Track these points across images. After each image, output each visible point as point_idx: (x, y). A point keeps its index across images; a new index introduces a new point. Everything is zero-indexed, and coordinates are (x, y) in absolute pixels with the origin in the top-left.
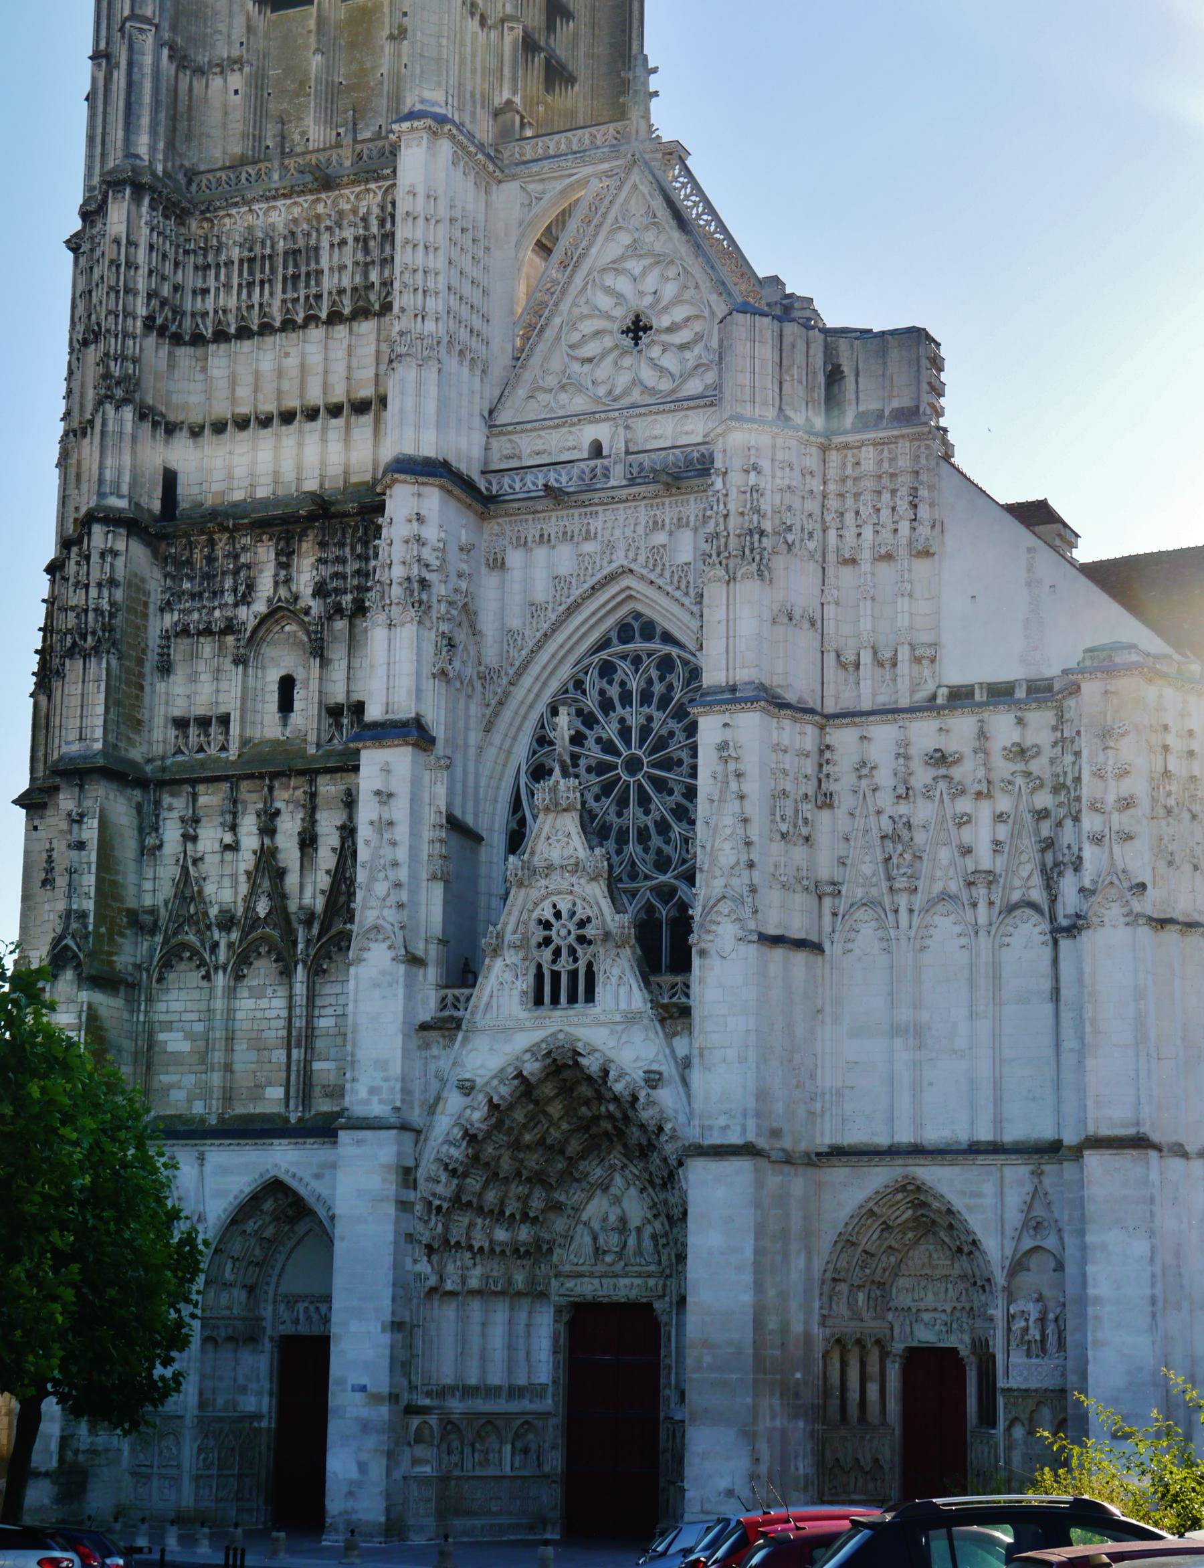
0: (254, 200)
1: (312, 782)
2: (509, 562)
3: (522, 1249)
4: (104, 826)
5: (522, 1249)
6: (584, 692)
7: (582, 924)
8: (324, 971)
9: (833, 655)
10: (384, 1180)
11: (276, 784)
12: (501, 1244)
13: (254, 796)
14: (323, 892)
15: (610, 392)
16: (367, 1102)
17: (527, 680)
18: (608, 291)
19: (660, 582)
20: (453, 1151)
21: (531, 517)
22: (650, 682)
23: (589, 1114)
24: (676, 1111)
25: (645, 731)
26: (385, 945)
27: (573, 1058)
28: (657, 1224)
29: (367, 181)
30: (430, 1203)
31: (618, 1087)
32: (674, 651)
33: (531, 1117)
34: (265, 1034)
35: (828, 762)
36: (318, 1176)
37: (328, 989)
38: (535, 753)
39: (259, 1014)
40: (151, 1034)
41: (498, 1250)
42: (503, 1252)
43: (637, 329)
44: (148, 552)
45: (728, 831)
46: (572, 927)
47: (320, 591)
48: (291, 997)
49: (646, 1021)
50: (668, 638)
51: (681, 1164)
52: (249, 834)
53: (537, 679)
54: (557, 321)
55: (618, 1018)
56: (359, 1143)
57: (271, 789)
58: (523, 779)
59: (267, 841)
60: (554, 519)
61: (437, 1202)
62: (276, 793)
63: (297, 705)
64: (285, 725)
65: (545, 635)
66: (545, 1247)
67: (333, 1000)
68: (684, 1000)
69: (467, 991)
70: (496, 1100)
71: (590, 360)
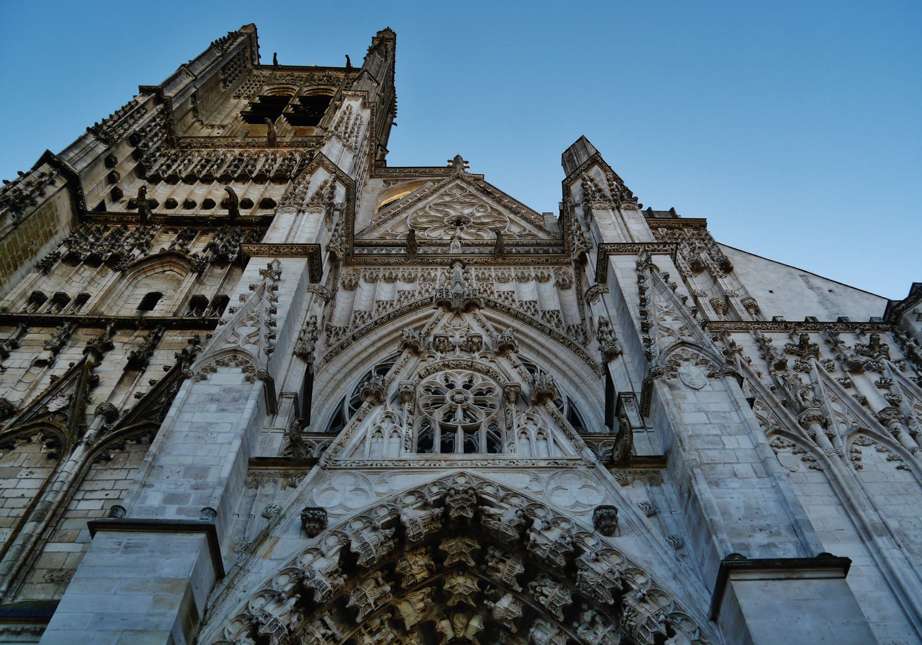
0: (218, 146)
10: (157, 601)
17: (365, 342)
18: (438, 211)
20: (271, 608)
23: (450, 634)
24: (649, 563)
26: (239, 370)
29: (298, 147)
37: (107, 475)
43: (459, 222)
44: (70, 216)
46: (472, 396)
49: (582, 469)
53: (373, 344)
54: (404, 215)
55: (543, 464)
60: (401, 270)
67: (108, 486)
70: (355, 546)
71: (425, 229)
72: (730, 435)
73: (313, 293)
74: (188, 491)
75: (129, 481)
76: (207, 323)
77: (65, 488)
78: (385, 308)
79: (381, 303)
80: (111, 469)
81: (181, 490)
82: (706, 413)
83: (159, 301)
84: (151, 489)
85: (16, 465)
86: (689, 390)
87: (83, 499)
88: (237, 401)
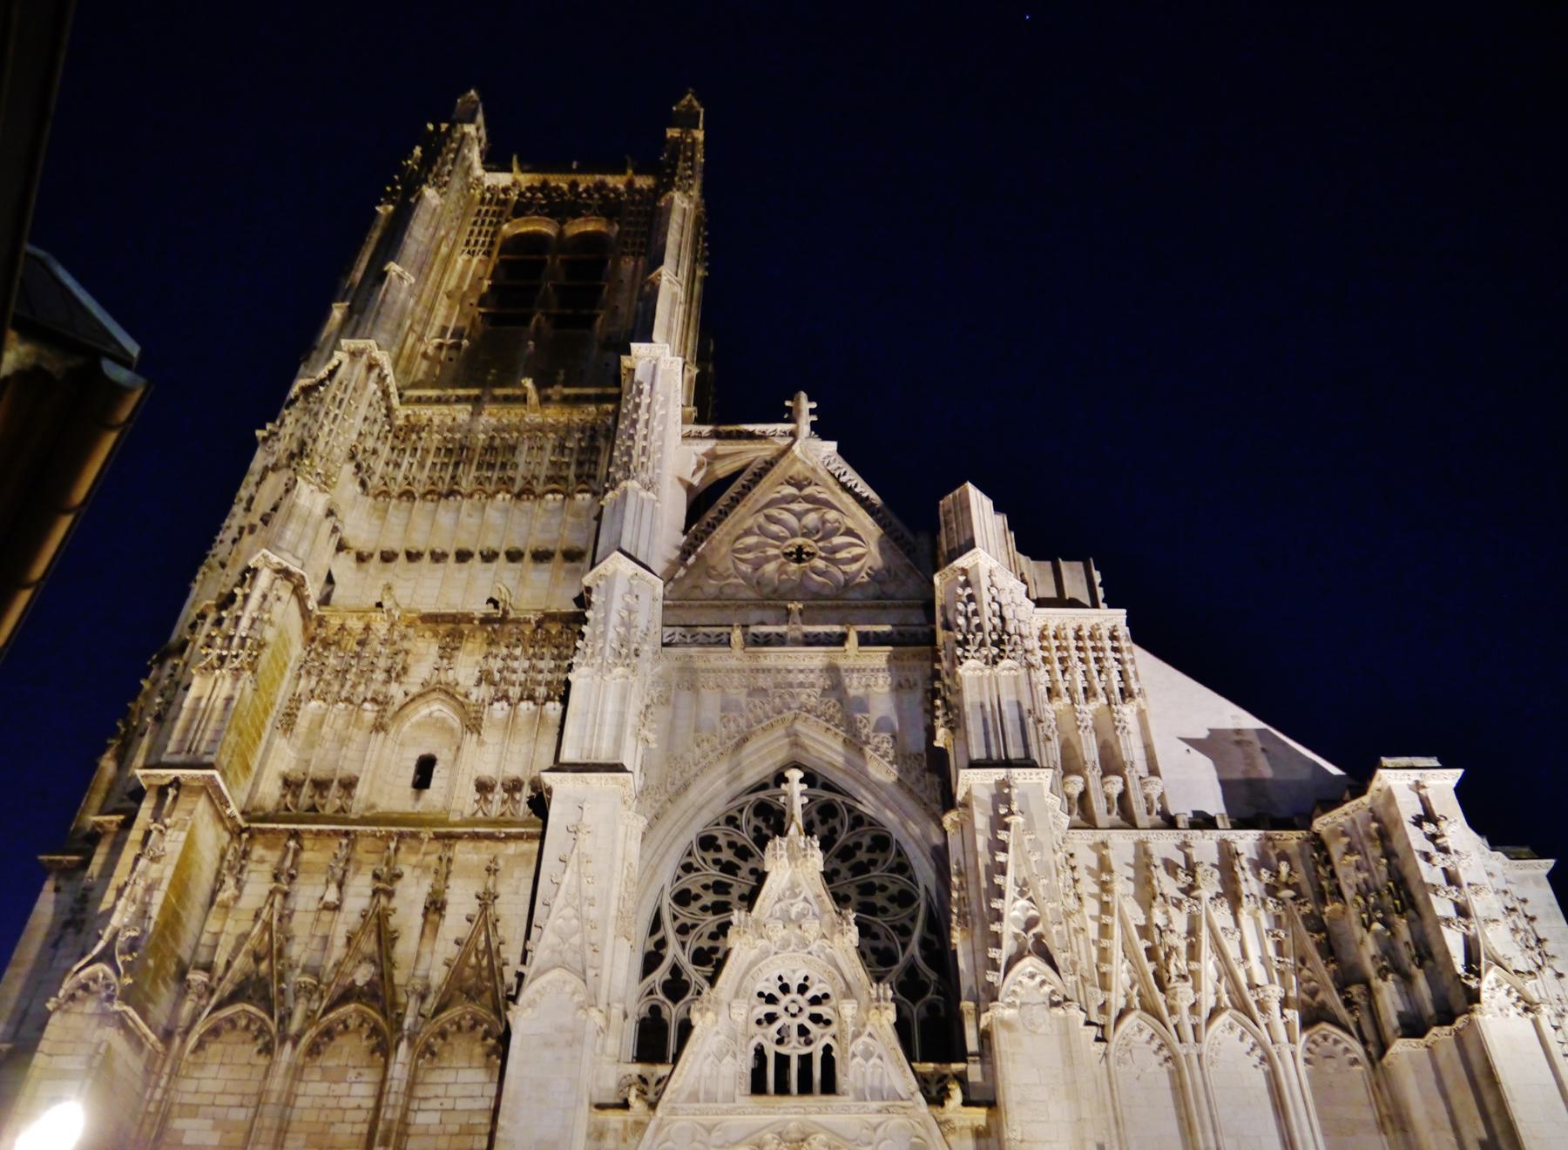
1: (450, 847)
4: (190, 843)
6: (738, 827)
11: (403, 848)
13: (374, 857)
34: (333, 1130)
37: (435, 1077)
38: (679, 878)
39: (331, 1103)
40: (166, 1118)
47: (485, 678)
48: (383, 1081)
52: (358, 895)
57: (397, 850)
58: (667, 900)
59: (383, 900)
62: (401, 855)
63: (434, 782)
64: (417, 798)
83: (435, 770)
85: (342, 1062)
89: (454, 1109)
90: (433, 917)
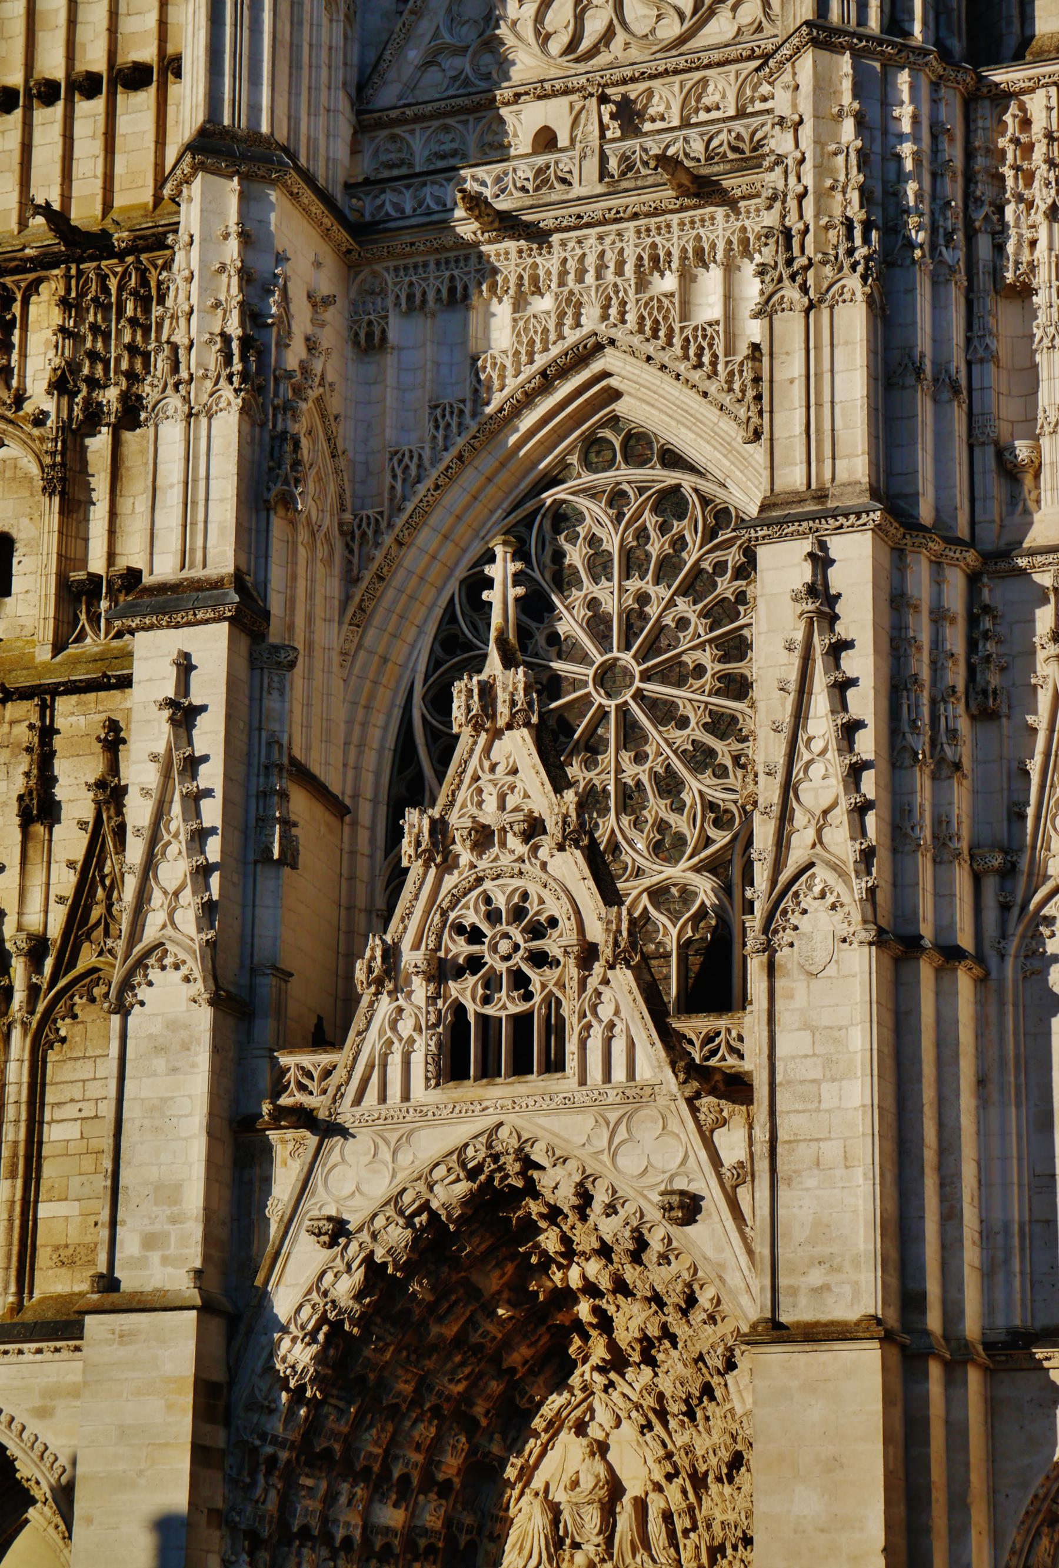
1: (46, 709)
2: (392, 335)
3: (422, 1543)
5: (422, 1543)
7: (536, 931)
8: (63, 1040)
9: (991, 450)
12: (387, 1530)
14: (61, 900)
15: (571, 47)
16: (140, 1263)
19: (665, 357)
21: (431, 260)
22: (642, 535)
25: (633, 621)
27: (523, 1173)
28: (673, 1491)
30: (255, 1450)
31: (609, 1228)
32: (687, 481)
33: (441, 1291)
35: (986, 636)
36: (43, 1413)
41: (378, 1543)
42: (387, 1547)
45: (817, 746)
47: (60, 385)
50: (672, 459)
51: (731, 1365)
56: (123, 1338)
61: (269, 1450)
63: (17, 584)
65: (460, 457)
66: (463, 1539)
68: (731, 1061)
69: (325, 1059)
72: (834, 1080)
73: (262, 669)
74: (168, 1227)
75: (100, 1083)
76: (113, 681)
77: (24, 1116)
78: (448, 425)
79: (439, 411)
80: (70, 1059)
81: (157, 1227)
82: (813, 1030)
83: (15, 561)
84: (125, 1228)
86: (803, 977)
87: (53, 1121)
88: (188, 1049)
89: (96, 1117)
90: (39, 829)
